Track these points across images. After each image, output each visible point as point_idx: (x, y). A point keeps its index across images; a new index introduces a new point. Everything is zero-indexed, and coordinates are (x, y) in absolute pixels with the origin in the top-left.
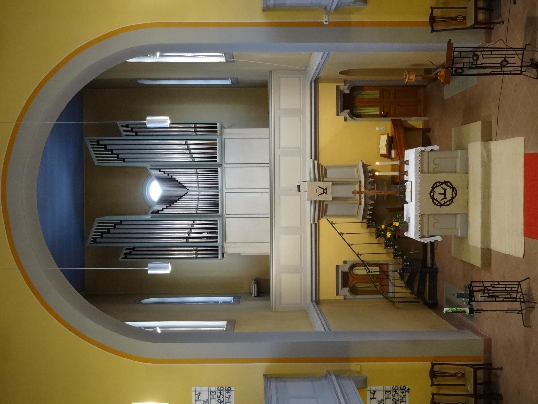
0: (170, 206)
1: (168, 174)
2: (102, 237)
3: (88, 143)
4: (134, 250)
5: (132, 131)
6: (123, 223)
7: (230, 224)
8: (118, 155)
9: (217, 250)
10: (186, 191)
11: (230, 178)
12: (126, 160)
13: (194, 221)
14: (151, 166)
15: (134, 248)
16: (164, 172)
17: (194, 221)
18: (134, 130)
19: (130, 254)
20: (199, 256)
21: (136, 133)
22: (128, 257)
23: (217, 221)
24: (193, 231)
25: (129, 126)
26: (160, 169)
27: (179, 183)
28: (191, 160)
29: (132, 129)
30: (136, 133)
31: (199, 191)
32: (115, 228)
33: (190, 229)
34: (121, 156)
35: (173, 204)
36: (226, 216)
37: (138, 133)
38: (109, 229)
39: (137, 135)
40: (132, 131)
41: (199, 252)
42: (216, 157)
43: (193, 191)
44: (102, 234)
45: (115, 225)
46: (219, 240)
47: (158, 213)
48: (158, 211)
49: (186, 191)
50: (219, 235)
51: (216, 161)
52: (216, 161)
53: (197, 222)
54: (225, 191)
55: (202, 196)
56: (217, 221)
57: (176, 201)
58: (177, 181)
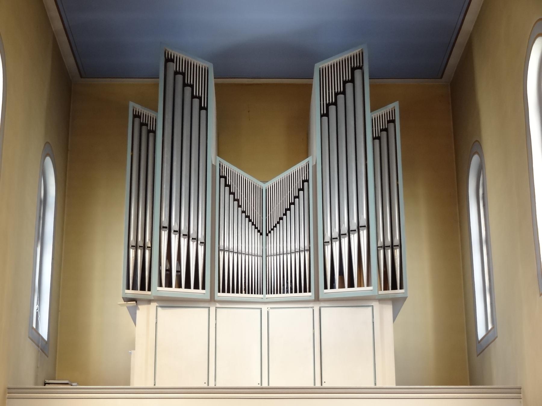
2: (176, 73)
3: (356, 51)
4: (149, 131)
5: (382, 130)
6: (203, 112)
9: (143, 288)
12: (325, 119)
13: (204, 243)
14: (315, 167)
15: (154, 132)
16: (303, 189)
17: (204, 243)
18: (384, 133)
19: (142, 124)
20: (132, 252)
21: (379, 138)
22: (137, 120)
23: (204, 288)
24: (184, 241)
25: (392, 125)
26: (307, 181)
29: (386, 130)
30: (379, 138)
31: (265, 256)
33: (188, 236)
34: (332, 108)
35: (239, 206)
38: (192, 86)
39: (374, 139)
40: (382, 130)
41: (139, 251)
46: (164, 290)
47: (221, 177)
50: (174, 291)
53: (201, 249)
55: (255, 262)
56: (204, 288)
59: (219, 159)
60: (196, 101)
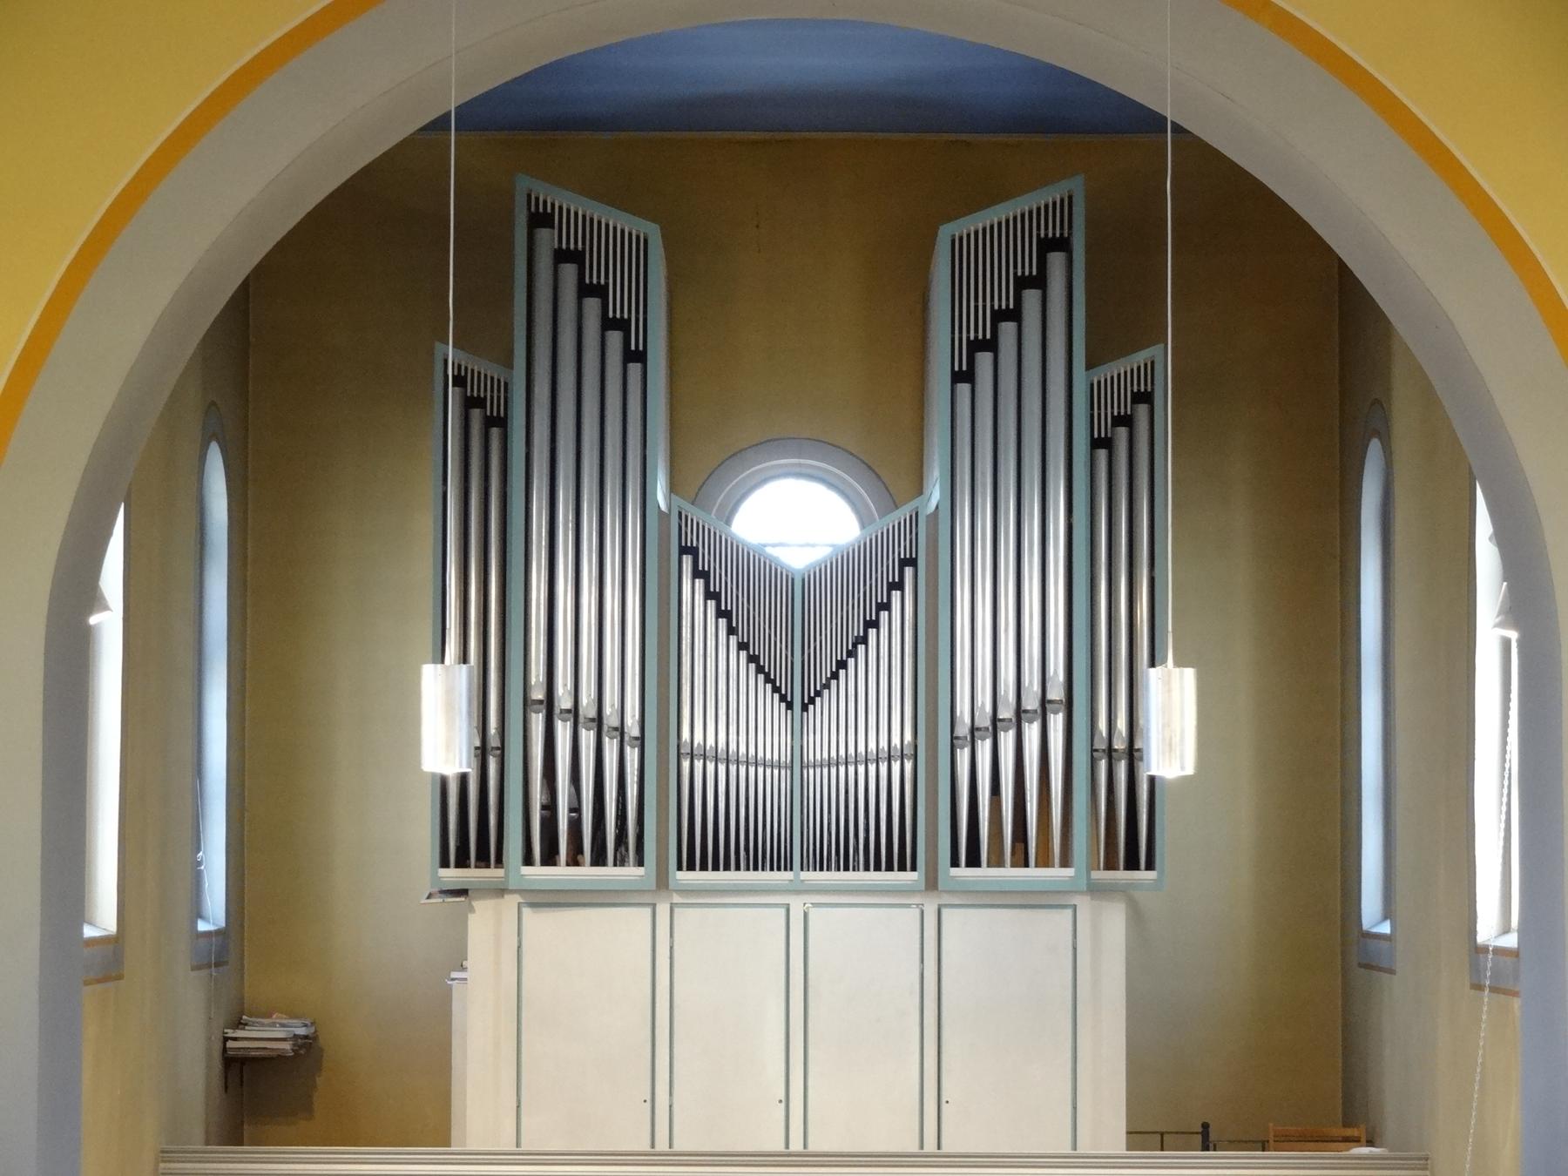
0: (720, 613)
1: (887, 606)
2: (561, 256)
4: (489, 422)
6: (635, 369)
7: (625, 929)
8: (991, 345)
10: (800, 699)
11: (862, 932)
12: (964, 389)
15: (502, 422)
16: (899, 586)
18: (1122, 432)
19: (470, 403)
26: (912, 562)
27: (842, 664)
28: (963, 730)
29: (1126, 421)
32: (608, 324)
34: (984, 360)
35: (731, 631)
36: (663, 910)
37: (1102, 454)
39: (1097, 443)
42: (973, 861)
43: (798, 733)
44: (576, 257)
45: (622, 325)
47: (684, 550)
48: (693, 551)
49: (800, 699)
51: (955, 863)
52: (955, 863)
54: (797, 904)
57: (742, 646)
58: (852, 653)
59: (679, 502)
60: (615, 338)
